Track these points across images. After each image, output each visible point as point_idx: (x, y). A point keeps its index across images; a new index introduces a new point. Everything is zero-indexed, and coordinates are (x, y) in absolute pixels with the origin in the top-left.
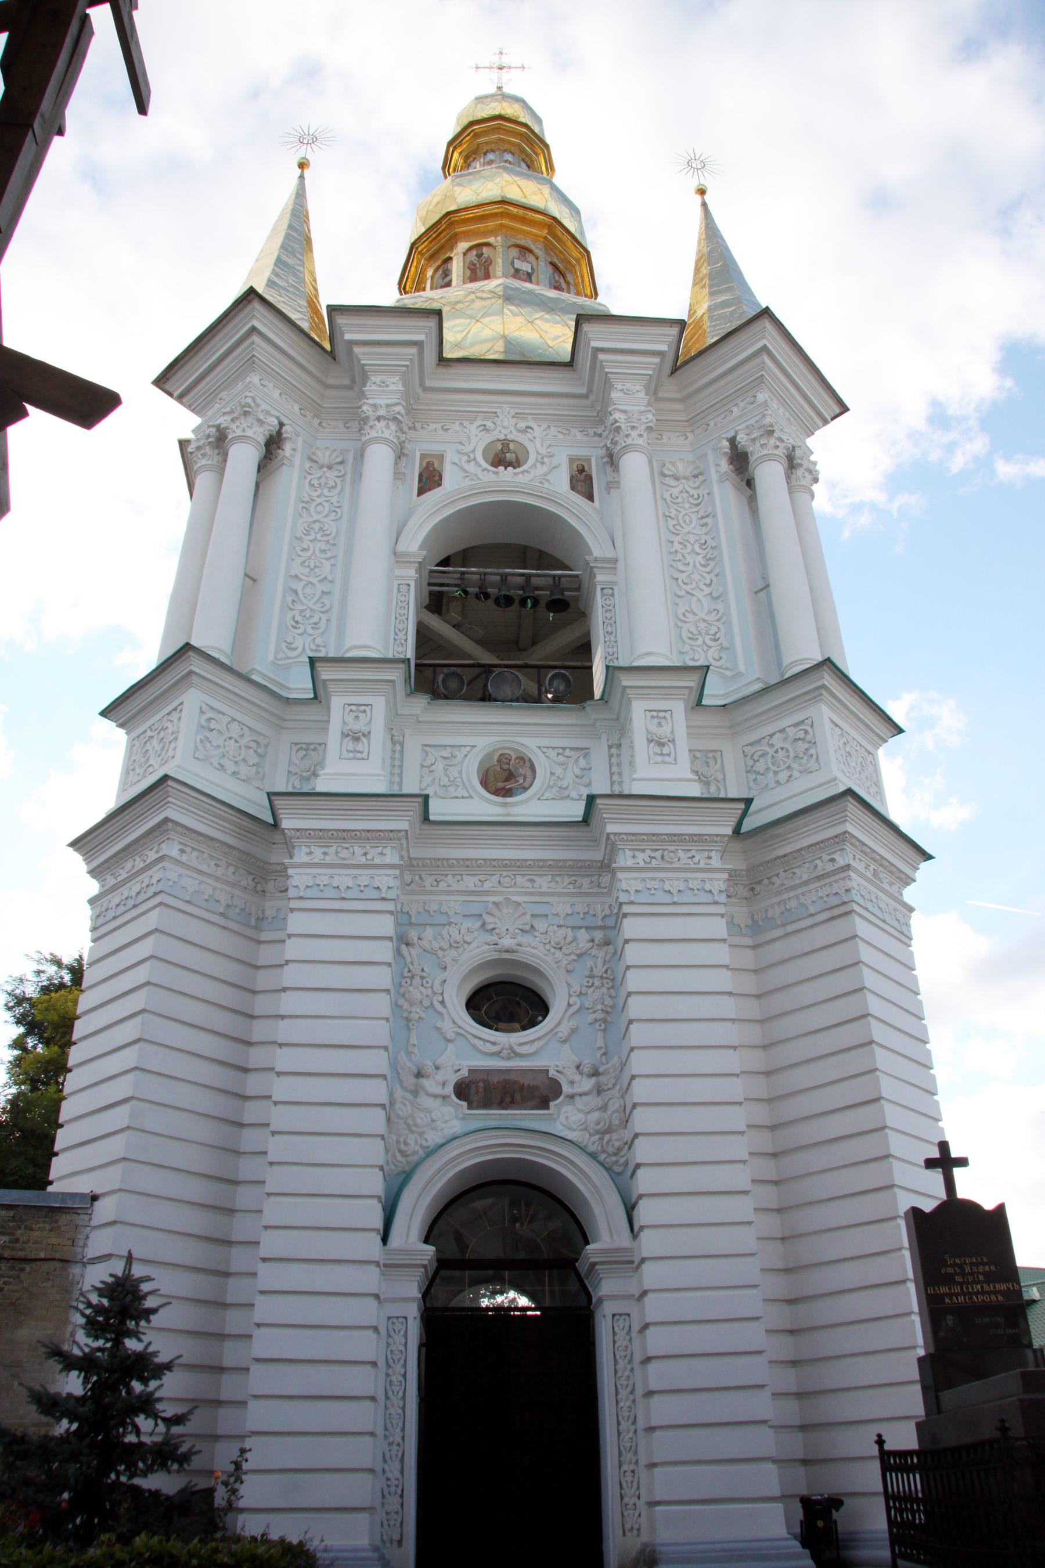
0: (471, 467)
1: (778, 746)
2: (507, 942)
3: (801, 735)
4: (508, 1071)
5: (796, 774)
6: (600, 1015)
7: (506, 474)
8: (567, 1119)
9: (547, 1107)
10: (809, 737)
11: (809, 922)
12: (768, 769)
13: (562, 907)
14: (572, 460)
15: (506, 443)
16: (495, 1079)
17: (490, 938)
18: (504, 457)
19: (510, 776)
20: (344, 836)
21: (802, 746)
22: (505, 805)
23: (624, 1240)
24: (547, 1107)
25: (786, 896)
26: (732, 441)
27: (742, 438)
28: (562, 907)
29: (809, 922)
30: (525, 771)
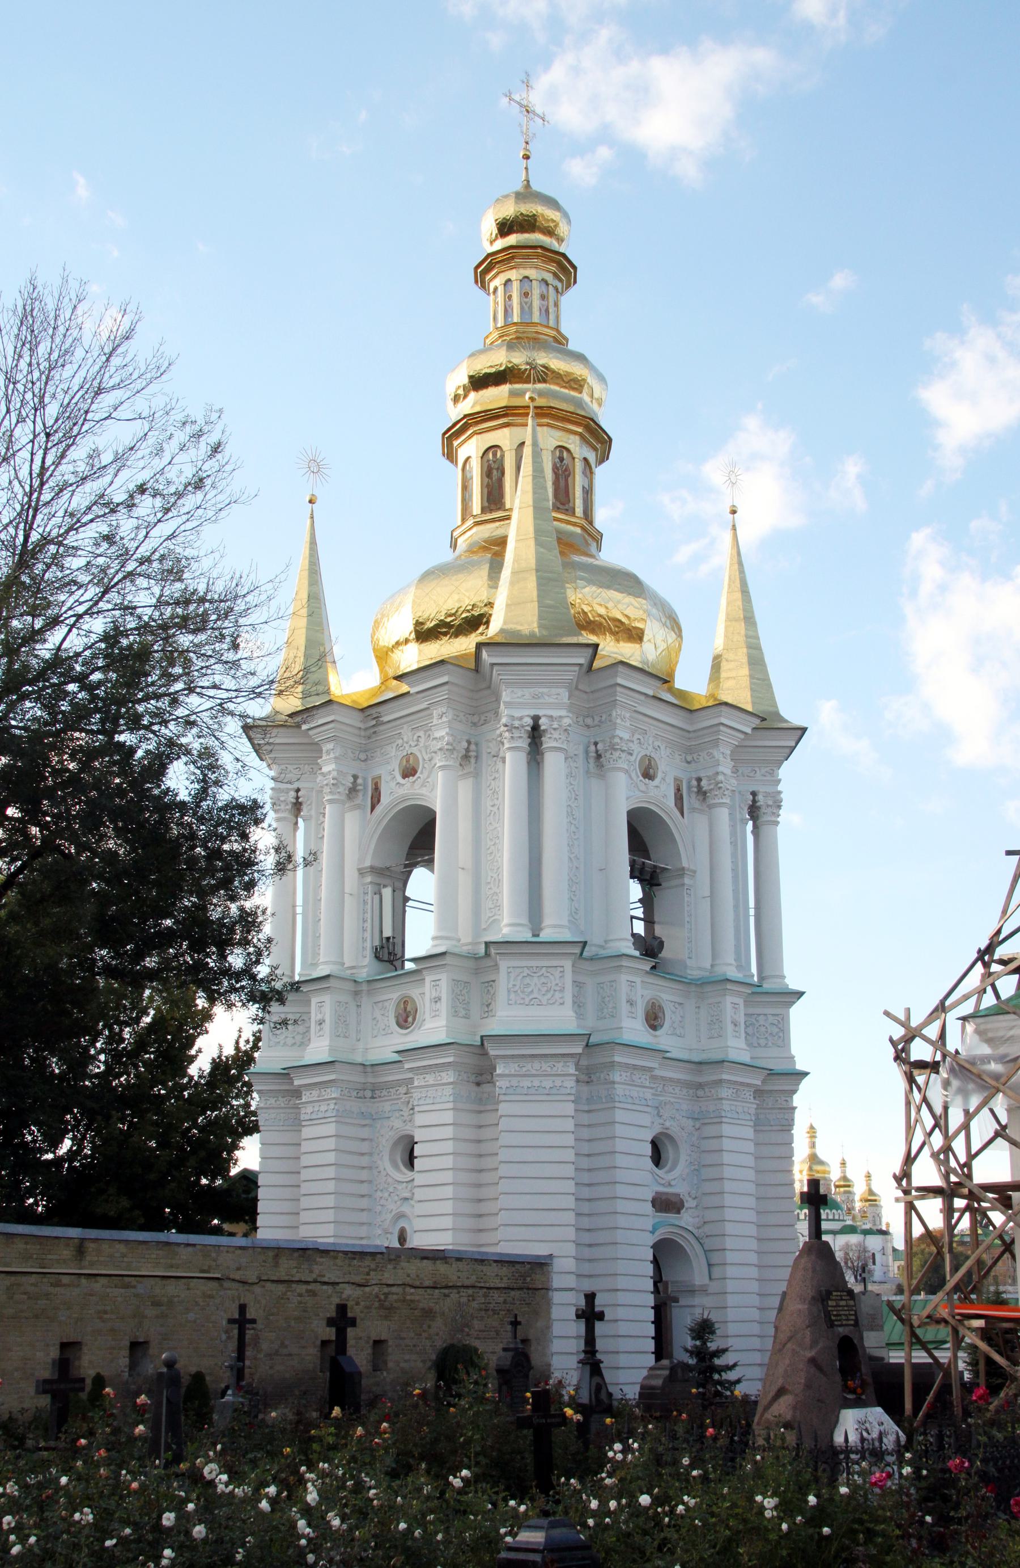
0: (633, 775)
1: (762, 1023)
2: (667, 1124)
3: (776, 1022)
4: (667, 1194)
5: (770, 1044)
6: (696, 1167)
8: (686, 1219)
9: (678, 1212)
10: (780, 1026)
11: (770, 1128)
12: (754, 1034)
13: (684, 1107)
14: (676, 779)
15: (650, 759)
16: (664, 1197)
17: (661, 1121)
19: (656, 1018)
20: (635, 1067)
21: (775, 1030)
22: (656, 1036)
23: (706, 1281)
24: (678, 1212)
25: (759, 1111)
27: (760, 797)
28: (684, 1107)
29: (770, 1128)
30: (661, 1015)
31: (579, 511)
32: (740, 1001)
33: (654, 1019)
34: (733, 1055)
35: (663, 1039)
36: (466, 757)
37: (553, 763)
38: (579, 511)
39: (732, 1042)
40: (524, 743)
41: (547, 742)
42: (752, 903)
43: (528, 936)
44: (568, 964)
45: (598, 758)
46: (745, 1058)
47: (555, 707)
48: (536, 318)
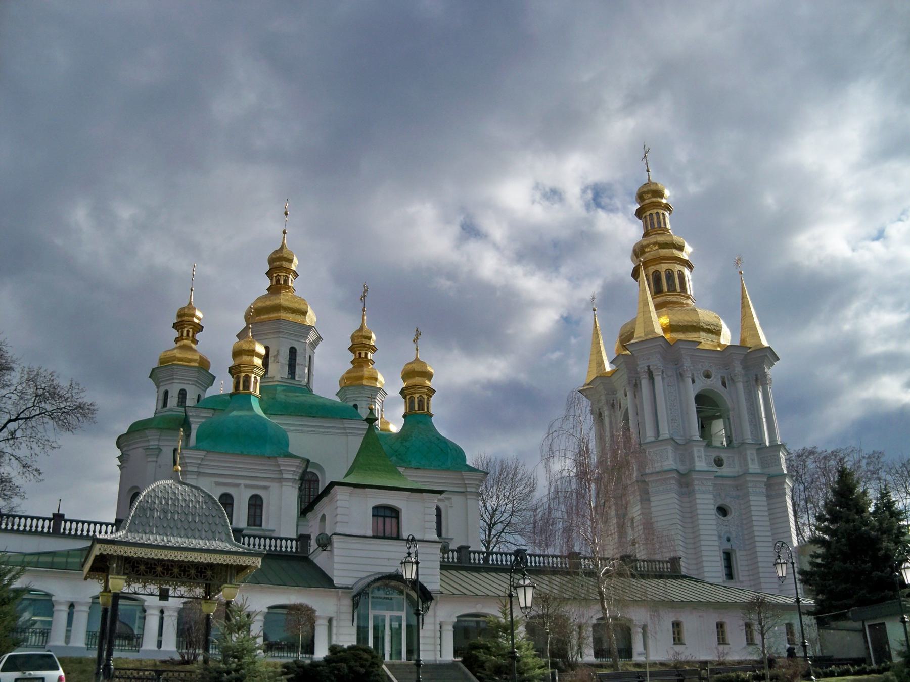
7: (708, 380)
15: (708, 371)
18: (708, 376)
26: (756, 375)
31: (679, 290)
32: (755, 452)
33: (719, 463)
34: (751, 471)
35: (725, 471)
36: (636, 385)
37: (658, 380)
38: (679, 290)
39: (751, 466)
40: (647, 376)
41: (654, 374)
42: (763, 416)
43: (653, 439)
44: (670, 447)
45: (681, 376)
46: (759, 471)
47: (656, 362)
48: (656, 226)
